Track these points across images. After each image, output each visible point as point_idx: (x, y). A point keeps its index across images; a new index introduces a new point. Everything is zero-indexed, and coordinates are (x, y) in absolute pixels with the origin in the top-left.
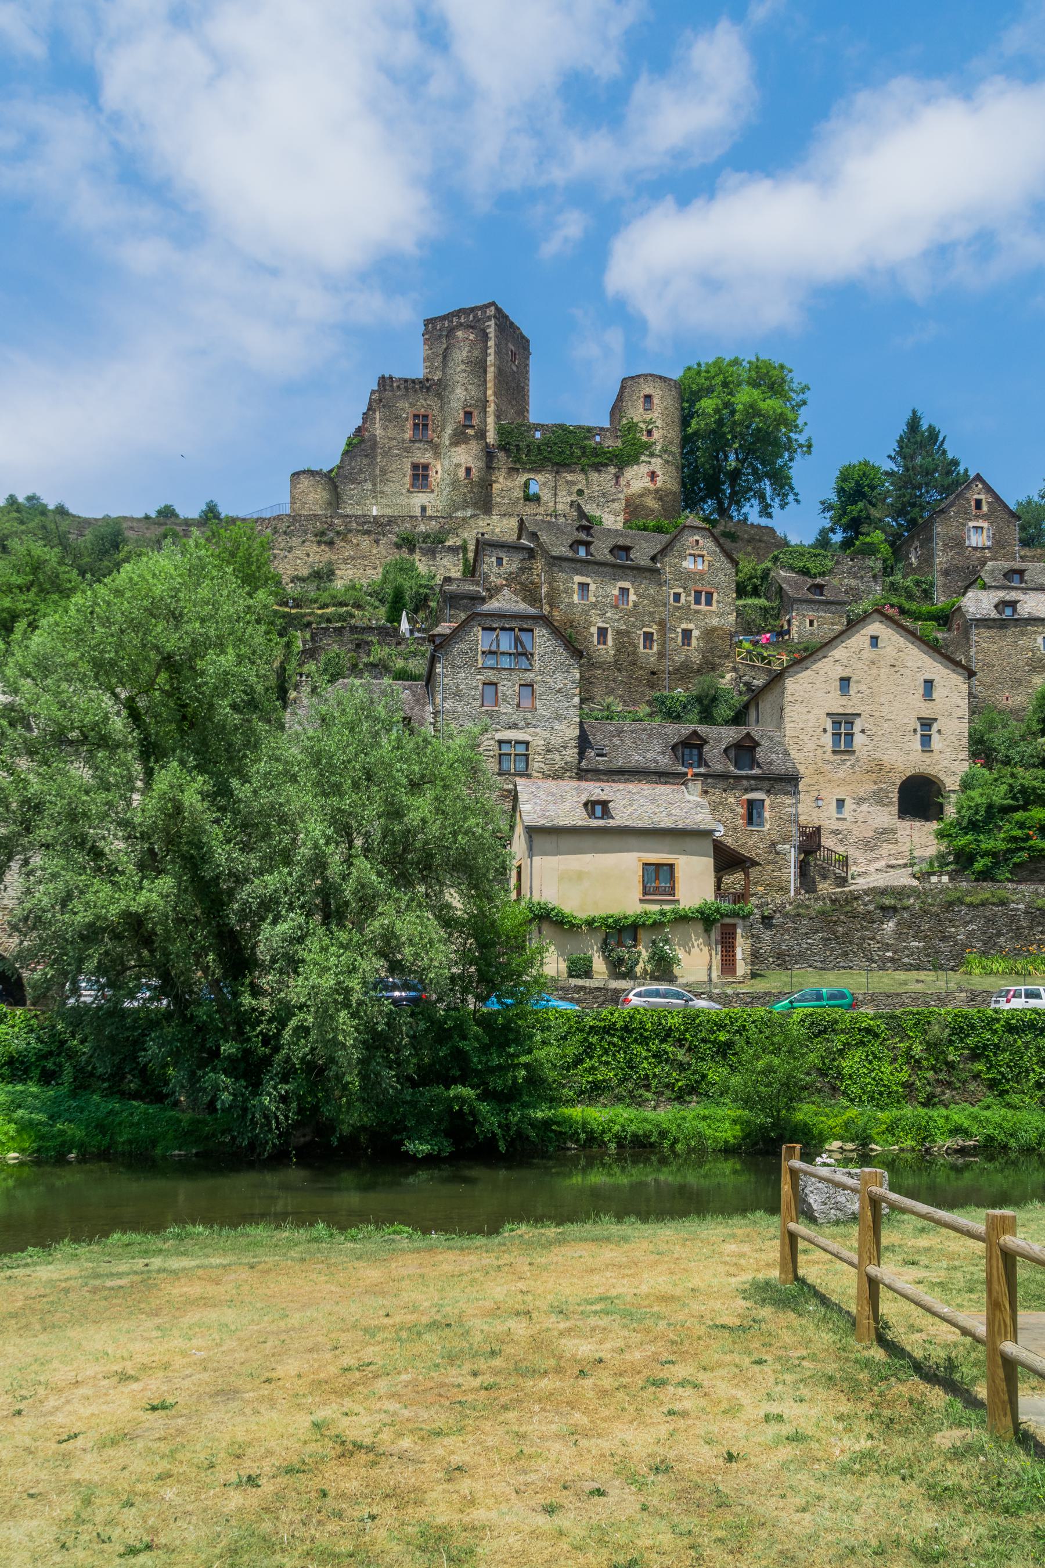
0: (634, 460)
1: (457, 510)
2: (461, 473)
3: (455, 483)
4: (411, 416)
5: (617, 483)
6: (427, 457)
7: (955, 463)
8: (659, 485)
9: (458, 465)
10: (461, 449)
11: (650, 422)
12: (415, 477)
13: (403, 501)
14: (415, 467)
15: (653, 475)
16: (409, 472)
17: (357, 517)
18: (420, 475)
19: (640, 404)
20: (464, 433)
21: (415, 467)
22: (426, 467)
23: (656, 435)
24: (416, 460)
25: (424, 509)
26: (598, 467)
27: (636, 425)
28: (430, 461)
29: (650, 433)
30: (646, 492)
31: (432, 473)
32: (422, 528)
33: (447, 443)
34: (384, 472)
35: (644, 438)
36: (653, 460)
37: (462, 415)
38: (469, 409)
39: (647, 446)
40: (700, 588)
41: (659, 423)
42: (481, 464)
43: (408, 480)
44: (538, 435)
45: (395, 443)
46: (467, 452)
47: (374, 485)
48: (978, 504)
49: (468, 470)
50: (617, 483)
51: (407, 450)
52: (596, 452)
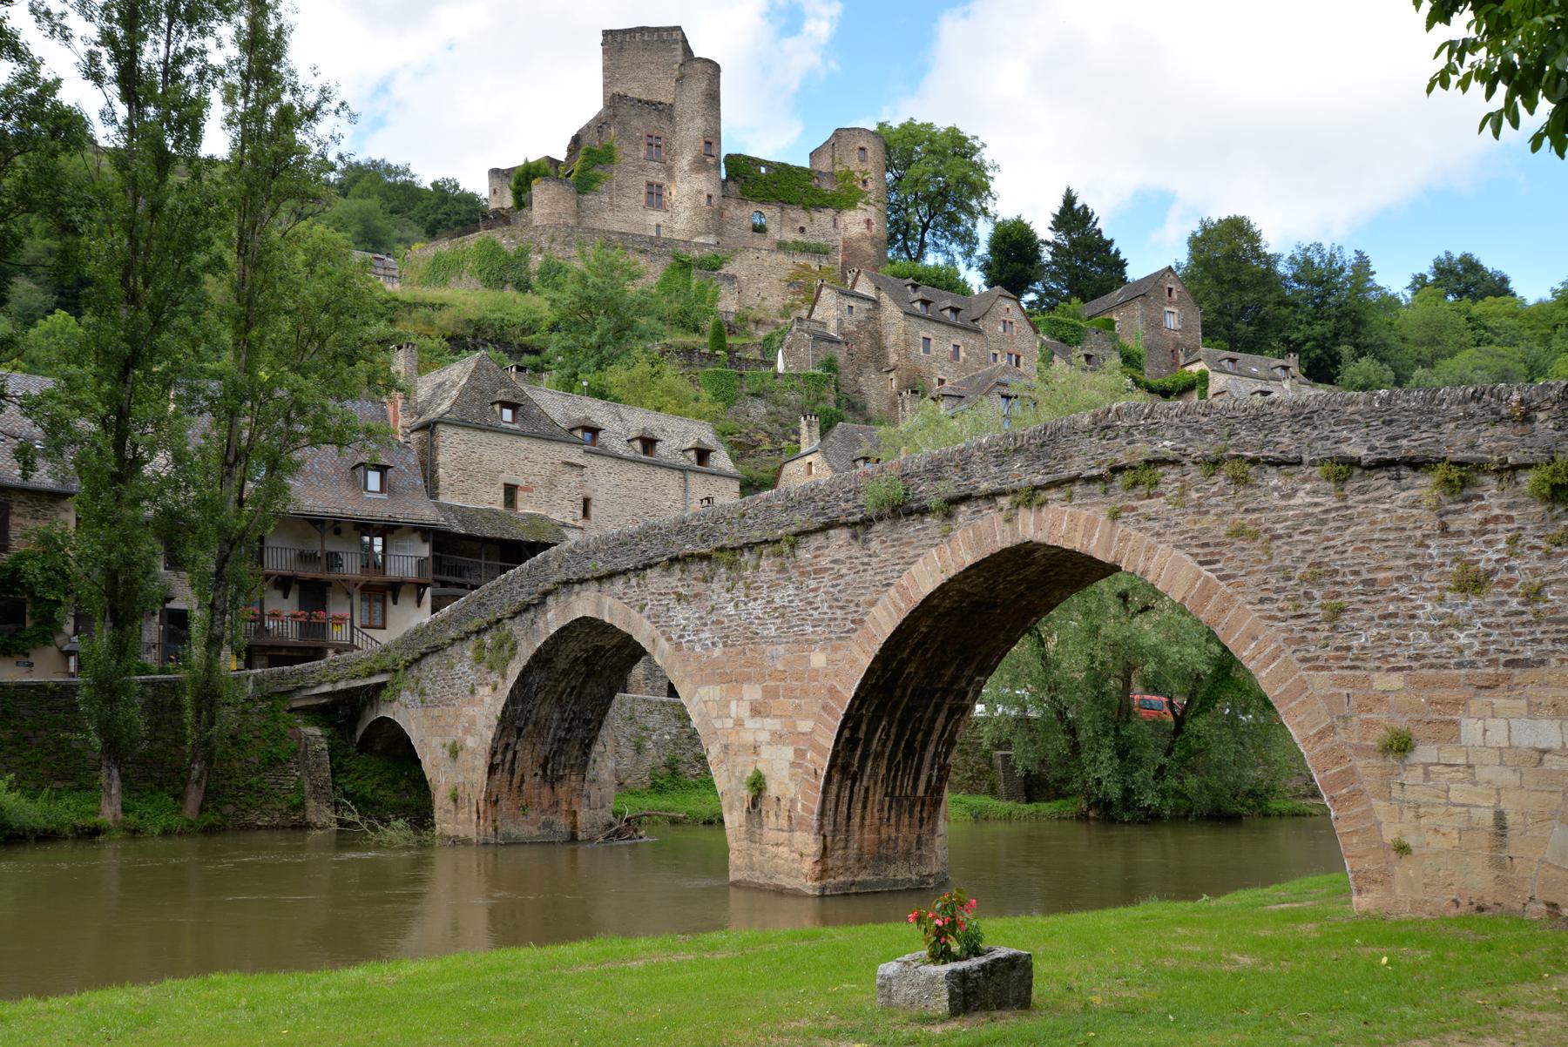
0: (852, 205)
1: (700, 234)
2: (703, 199)
3: (697, 206)
4: (644, 136)
5: (835, 226)
6: (660, 178)
7: (1111, 242)
8: (874, 232)
9: (700, 192)
10: (702, 176)
11: (865, 173)
12: (650, 193)
13: (637, 217)
14: (650, 185)
15: (868, 222)
16: (644, 191)
17: (634, 235)
18: (655, 196)
19: (856, 155)
20: (705, 161)
21: (650, 185)
22: (660, 186)
23: (871, 186)
24: (651, 180)
25: (658, 226)
26: (819, 207)
27: (852, 173)
28: (665, 182)
29: (865, 182)
30: (863, 238)
31: (666, 194)
32: (696, 253)
33: (686, 168)
34: (619, 187)
35: (860, 187)
36: (869, 208)
37: (702, 143)
38: (708, 139)
39: (862, 195)
40: (1011, 351)
41: (873, 175)
42: (719, 193)
43: (642, 197)
44: (763, 170)
45: (630, 160)
46: (708, 180)
47: (611, 198)
48: (1170, 290)
49: (709, 197)
50: (835, 226)
51: (642, 168)
52: (816, 193)
